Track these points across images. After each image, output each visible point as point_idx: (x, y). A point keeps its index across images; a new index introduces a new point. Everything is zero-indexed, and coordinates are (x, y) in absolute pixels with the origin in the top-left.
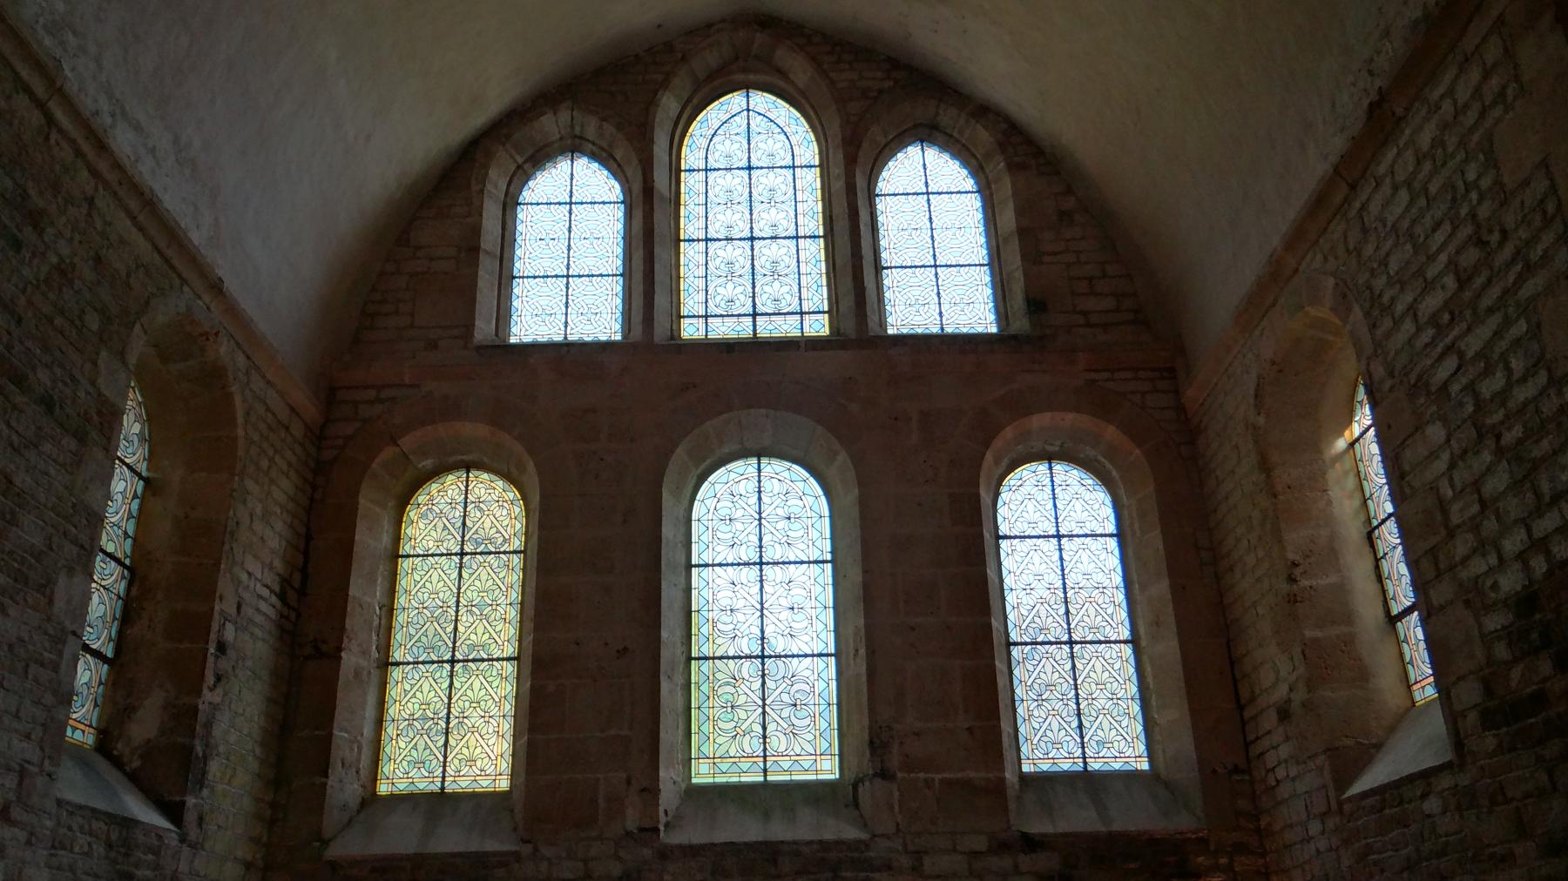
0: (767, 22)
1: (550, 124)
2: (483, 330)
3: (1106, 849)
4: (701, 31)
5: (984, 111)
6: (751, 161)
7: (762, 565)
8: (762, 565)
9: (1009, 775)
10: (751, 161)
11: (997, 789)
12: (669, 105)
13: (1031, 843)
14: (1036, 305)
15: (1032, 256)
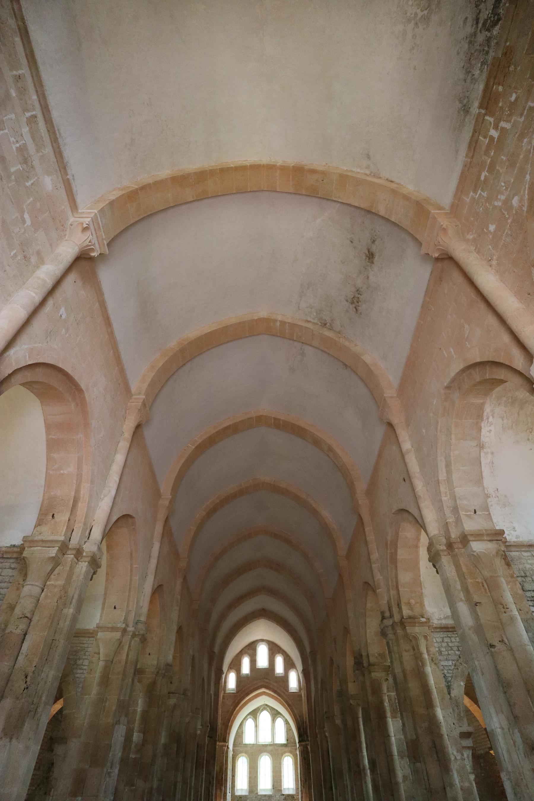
0: (266, 705)
1: (248, 717)
2: (244, 743)
3: (289, 795)
4: (261, 706)
5: (284, 717)
6: (265, 717)
7: (265, 763)
8: (265, 763)
9: (282, 789)
10: (265, 717)
11: (281, 790)
12: (258, 714)
13: (283, 795)
14: (287, 740)
15: (287, 734)
